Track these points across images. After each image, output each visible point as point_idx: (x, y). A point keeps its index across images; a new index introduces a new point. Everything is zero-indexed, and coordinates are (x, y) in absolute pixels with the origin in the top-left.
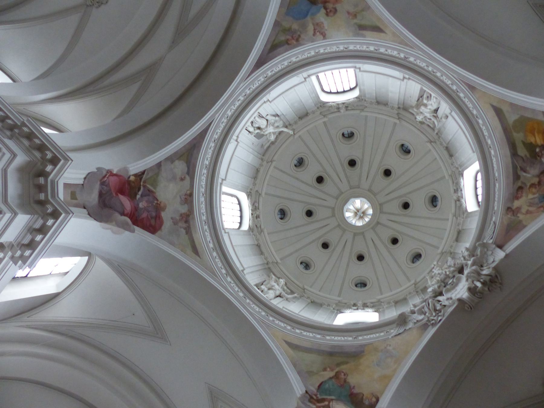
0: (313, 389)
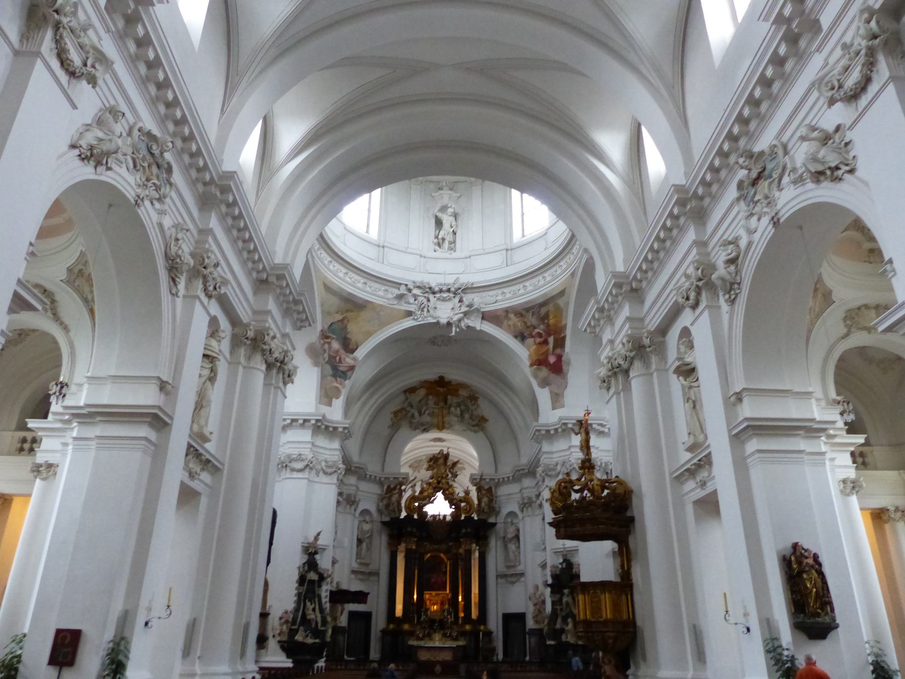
0: (326, 327)
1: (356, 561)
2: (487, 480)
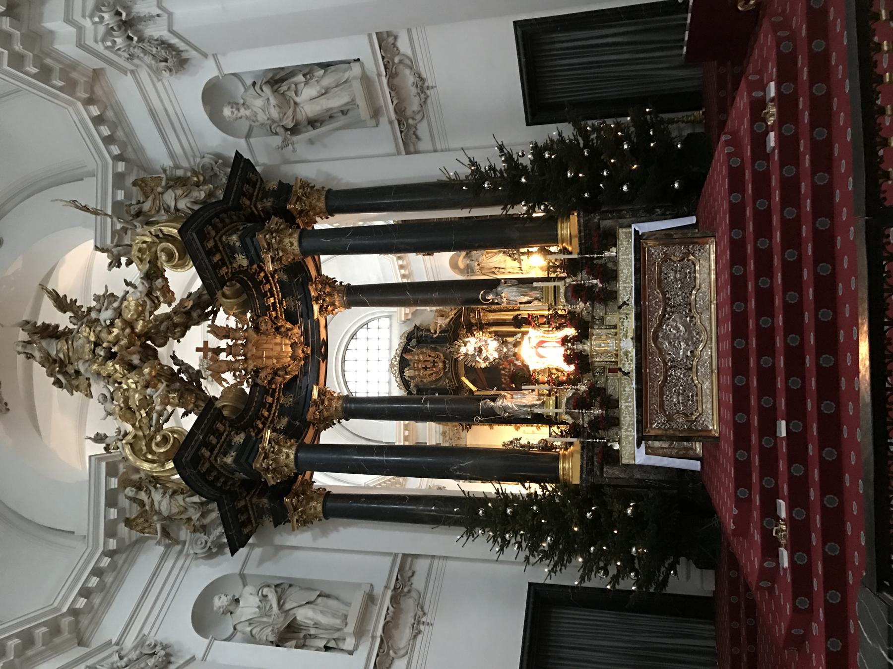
1: (351, 653)
2: (120, 195)
